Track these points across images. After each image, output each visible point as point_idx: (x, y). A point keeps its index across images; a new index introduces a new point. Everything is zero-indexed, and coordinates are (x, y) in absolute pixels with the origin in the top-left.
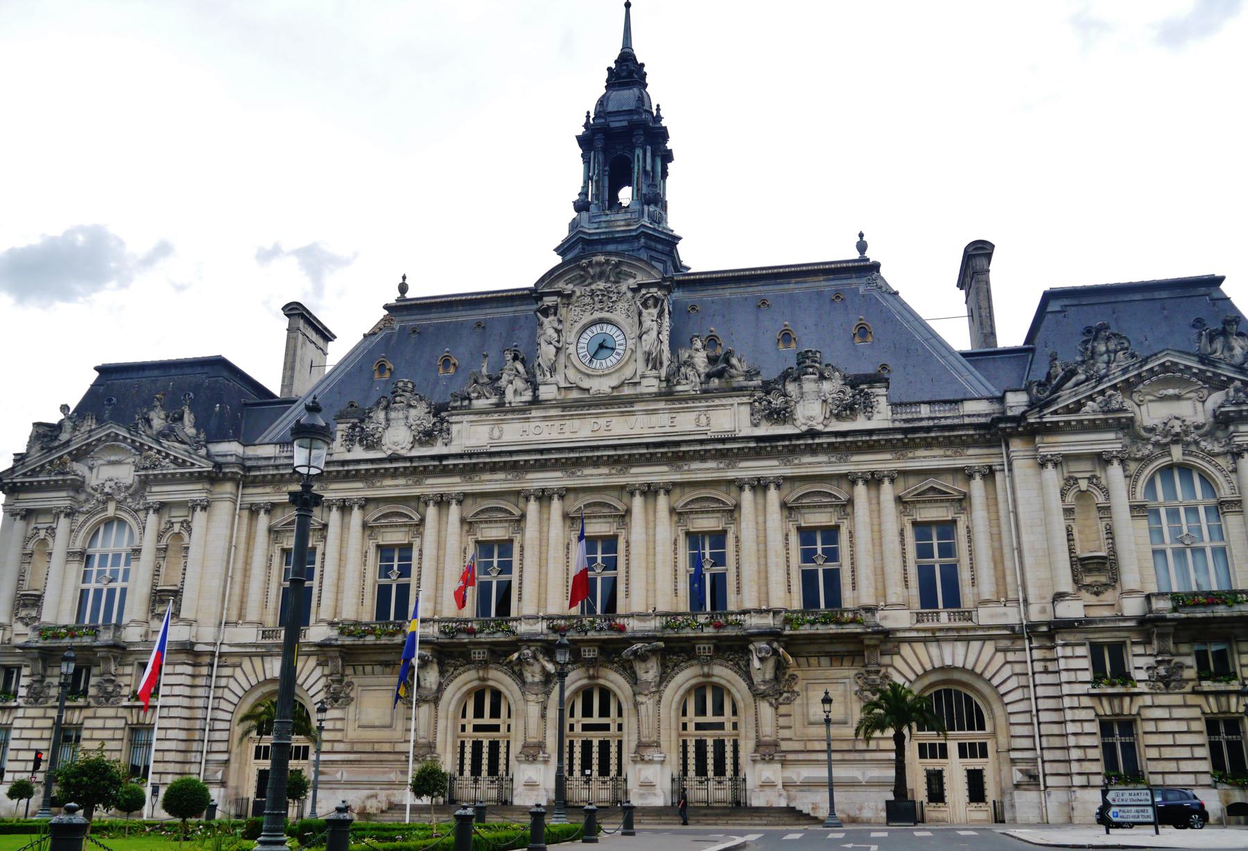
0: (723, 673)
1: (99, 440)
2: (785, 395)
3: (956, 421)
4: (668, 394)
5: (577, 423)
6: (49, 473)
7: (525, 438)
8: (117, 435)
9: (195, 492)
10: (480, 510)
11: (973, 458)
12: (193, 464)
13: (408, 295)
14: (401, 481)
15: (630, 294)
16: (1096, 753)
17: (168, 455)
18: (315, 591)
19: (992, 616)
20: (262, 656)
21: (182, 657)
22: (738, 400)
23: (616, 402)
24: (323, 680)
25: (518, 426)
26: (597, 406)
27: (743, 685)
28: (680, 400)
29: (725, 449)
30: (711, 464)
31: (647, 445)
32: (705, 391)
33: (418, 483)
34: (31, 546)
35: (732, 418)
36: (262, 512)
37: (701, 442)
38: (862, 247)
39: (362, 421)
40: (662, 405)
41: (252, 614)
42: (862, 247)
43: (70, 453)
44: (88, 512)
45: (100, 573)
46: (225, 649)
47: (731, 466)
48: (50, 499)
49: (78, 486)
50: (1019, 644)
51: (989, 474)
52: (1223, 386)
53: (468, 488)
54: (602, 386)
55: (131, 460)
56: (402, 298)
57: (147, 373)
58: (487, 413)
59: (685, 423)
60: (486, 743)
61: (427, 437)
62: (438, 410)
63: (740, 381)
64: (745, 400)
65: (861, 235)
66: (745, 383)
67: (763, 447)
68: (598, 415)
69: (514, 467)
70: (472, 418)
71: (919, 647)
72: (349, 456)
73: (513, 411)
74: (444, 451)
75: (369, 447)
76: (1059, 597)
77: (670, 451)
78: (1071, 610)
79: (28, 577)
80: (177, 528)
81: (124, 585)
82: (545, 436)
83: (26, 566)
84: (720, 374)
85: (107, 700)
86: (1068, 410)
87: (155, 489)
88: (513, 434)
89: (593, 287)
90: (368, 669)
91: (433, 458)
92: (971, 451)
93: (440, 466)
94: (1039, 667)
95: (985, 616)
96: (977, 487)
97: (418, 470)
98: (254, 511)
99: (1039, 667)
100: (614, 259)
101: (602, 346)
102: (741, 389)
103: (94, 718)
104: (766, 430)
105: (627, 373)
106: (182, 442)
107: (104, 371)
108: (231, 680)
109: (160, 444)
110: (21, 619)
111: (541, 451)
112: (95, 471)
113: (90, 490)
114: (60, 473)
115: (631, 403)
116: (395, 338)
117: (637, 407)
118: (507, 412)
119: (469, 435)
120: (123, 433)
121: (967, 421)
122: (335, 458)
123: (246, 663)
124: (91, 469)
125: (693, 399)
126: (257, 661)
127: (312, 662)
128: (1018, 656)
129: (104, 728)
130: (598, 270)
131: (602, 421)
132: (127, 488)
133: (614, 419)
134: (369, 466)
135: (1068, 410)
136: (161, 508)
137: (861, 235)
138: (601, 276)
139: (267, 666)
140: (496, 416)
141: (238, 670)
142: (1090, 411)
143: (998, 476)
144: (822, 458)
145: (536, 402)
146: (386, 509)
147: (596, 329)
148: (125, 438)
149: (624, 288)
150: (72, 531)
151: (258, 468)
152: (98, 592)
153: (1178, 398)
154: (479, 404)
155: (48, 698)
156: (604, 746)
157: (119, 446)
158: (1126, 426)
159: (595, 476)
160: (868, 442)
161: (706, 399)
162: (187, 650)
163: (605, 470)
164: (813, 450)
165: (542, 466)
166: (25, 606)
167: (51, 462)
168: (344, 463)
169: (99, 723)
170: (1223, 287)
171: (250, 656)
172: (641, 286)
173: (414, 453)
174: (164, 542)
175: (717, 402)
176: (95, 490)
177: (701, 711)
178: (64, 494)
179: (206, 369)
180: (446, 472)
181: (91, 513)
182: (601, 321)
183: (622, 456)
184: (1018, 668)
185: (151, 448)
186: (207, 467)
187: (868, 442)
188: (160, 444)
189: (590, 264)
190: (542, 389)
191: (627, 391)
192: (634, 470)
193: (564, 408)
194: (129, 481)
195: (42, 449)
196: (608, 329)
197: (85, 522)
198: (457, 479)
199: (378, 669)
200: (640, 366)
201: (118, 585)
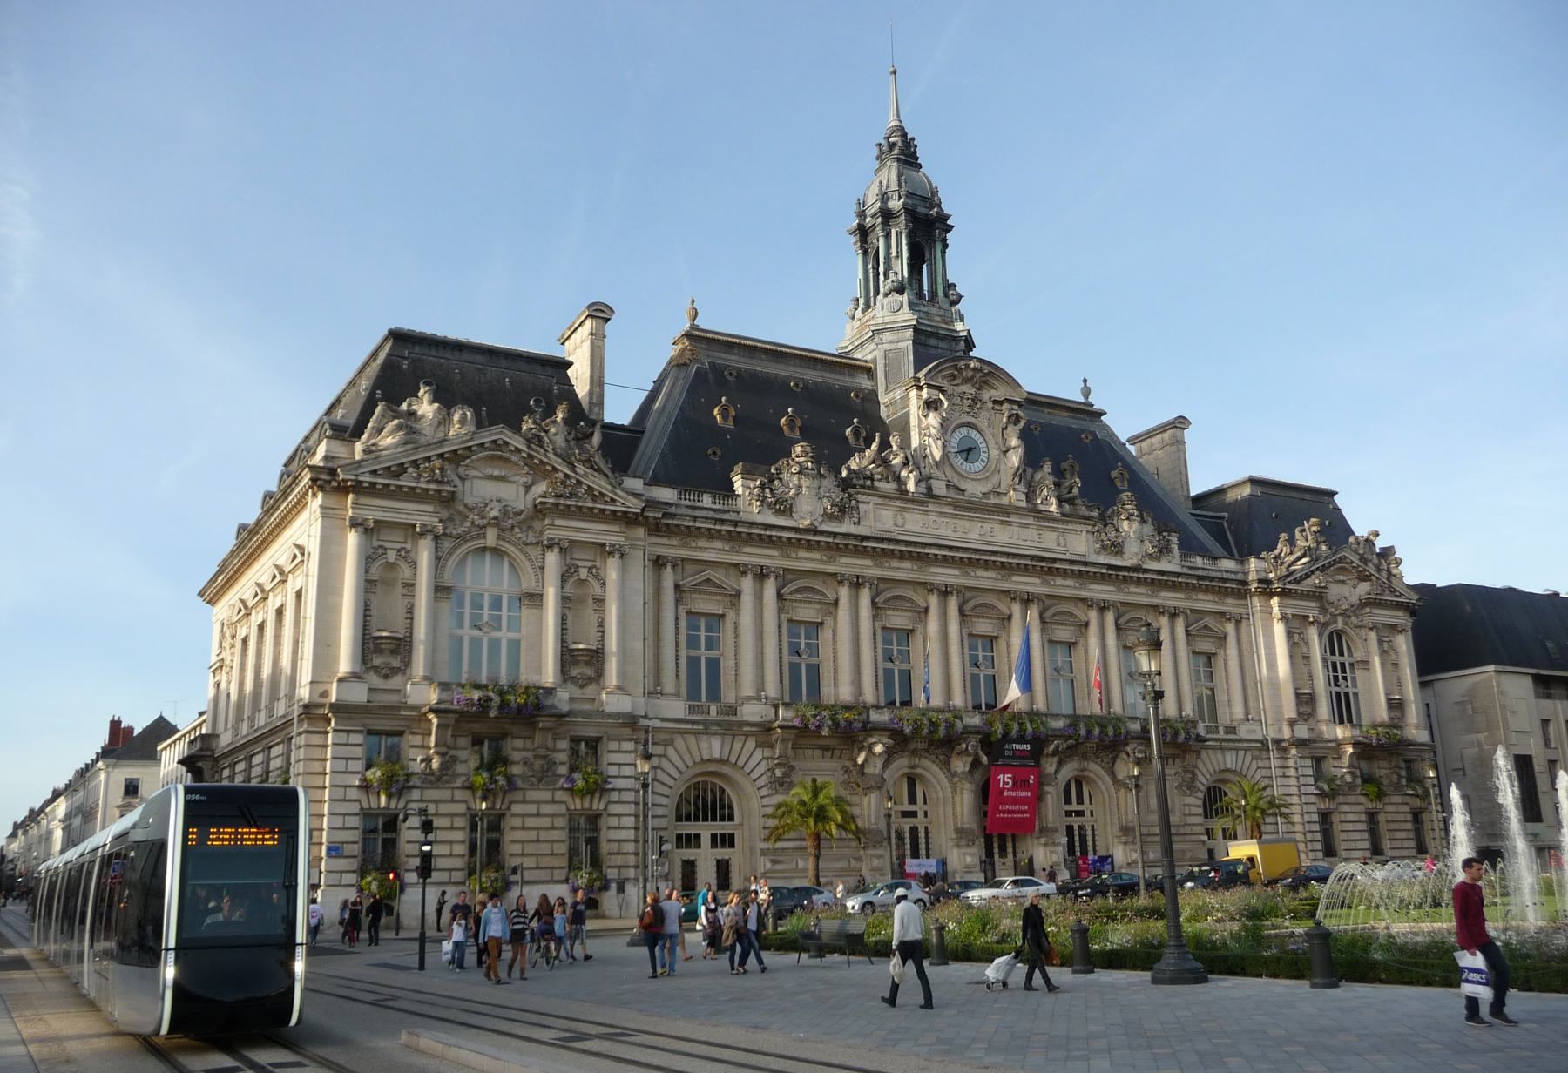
0: (1095, 769)
1: (482, 445)
2: (1117, 530)
3: (1219, 575)
4: (1036, 512)
5: (967, 524)
6: (418, 479)
7: (924, 530)
8: (506, 443)
9: (610, 534)
10: (884, 596)
11: (1230, 606)
12: (613, 500)
13: (702, 323)
14: (816, 555)
15: (990, 405)
16: (1318, 836)
17: (579, 482)
18: (727, 664)
19: (1249, 732)
20: (696, 734)
21: (627, 731)
22: (1085, 528)
23: (1004, 512)
24: (764, 763)
25: (918, 516)
26: (982, 511)
27: (1107, 779)
28: (1044, 519)
29: (1080, 571)
30: (1069, 582)
31: (1033, 558)
32: (1064, 515)
33: (831, 560)
34: (375, 570)
35: (1080, 543)
36: (669, 567)
37: (1072, 562)
38: (1086, 392)
39: (771, 481)
40: (1031, 521)
41: (669, 684)
42: (1086, 392)
43: (441, 456)
44: (459, 537)
45: (474, 617)
46: (657, 724)
47: (1082, 586)
48: (408, 512)
49: (449, 500)
50: (1264, 754)
51: (1238, 623)
52: (1363, 577)
53: (879, 573)
54: (975, 489)
55: (516, 478)
56: (693, 327)
57: (466, 356)
58: (890, 498)
59: (1046, 541)
60: (907, 829)
61: (842, 511)
62: (845, 485)
63: (1083, 511)
64: (1089, 528)
65: (1085, 381)
66: (1086, 513)
67: (1114, 575)
68: (983, 520)
69: (921, 558)
70: (877, 500)
71: (1211, 752)
72: (759, 519)
73: (913, 501)
74: (854, 530)
75: (779, 512)
76: (1292, 723)
77: (1044, 566)
78: (1302, 732)
79: (374, 612)
80: (583, 573)
81: (513, 635)
82: (941, 532)
83: (372, 597)
84: (1066, 501)
85: (540, 781)
86: (1297, 582)
87: (558, 522)
88: (917, 525)
89: (964, 388)
90: (809, 752)
91: (856, 537)
92: (1230, 601)
93: (859, 546)
94: (1280, 772)
95: (1243, 732)
96: (1230, 628)
97: (838, 546)
98: (659, 563)
99: (1280, 772)
100: (986, 369)
101: (969, 450)
102: (1088, 518)
103: (524, 802)
104: (1103, 559)
105: (995, 480)
106: (599, 470)
107: (399, 337)
108: (664, 760)
109: (573, 468)
110: (376, 669)
111: (950, 548)
112: (468, 483)
113: (461, 508)
114: (437, 481)
115: (1008, 514)
116: (710, 376)
117: (1013, 519)
118: (908, 501)
119: (876, 518)
120: (517, 442)
121: (1225, 575)
122: (743, 517)
123: (679, 742)
124: (463, 479)
125: (1054, 520)
126: (691, 739)
127: (751, 743)
128: (1266, 763)
129: (538, 815)
130: (970, 374)
131: (987, 526)
132: (517, 514)
133: (997, 527)
134: (792, 535)
135: (1297, 582)
136: (566, 548)
137: (1085, 381)
138: (967, 381)
139: (704, 745)
140: (898, 503)
141: (671, 751)
142: (1307, 585)
143: (1244, 623)
144: (1142, 590)
145: (930, 493)
146: (801, 583)
147: (964, 431)
148: (518, 450)
149: (987, 394)
150: (438, 559)
151: (674, 516)
152: (476, 644)
153: (1343, 582)
154: (882, 485)
155: (455, 776)
156: (914, 830)
157: (507, 460)
158: (1319, 596)
159: (985, 579)
160: (1165, 582)
161: (1063, 522)
162: (631, 721)
163: (992, 574)
164: (1139, 582)
165: (945, 561)
166: (378, 650)
167: (415, 463)
168: (752, 524)
169: (532, 809)
170: (1336, 498)
171: (682, 733)
172: (1008, 401)
173: (825, 528)
174: (567, 587)
175: (1070, 526)
176: (470, 510)
177: (1068, 801)
178: (430, 508)
179: (549, 371)
180: (860, 552)
181: (462, 538)
182: (969, 425)
183: (1008, 564)
184: (1264, 773)
185: (555, 470)
186: (635, 506)
187: (1165, 582)
188: (573, 468)
189: (967, 366)
190: (934, 483)
191: (993, 500)
192: (1015, 578)
193: (955, 507)
194: (520, 505)
195: (406, 443)
196: (974, 434)
197: (455, 548)
198: (868, 562)
199: (818, 753)
200: (1006, 479)
201: (504, 635)
